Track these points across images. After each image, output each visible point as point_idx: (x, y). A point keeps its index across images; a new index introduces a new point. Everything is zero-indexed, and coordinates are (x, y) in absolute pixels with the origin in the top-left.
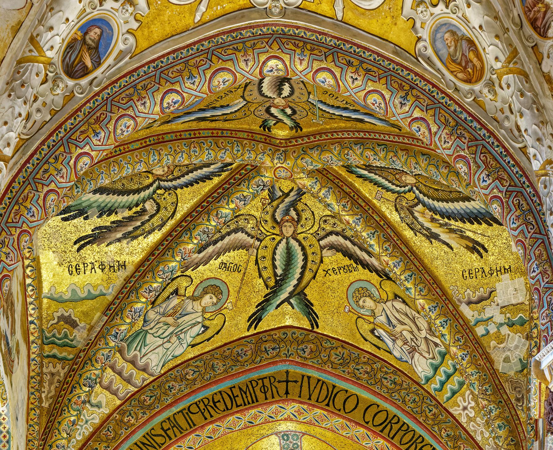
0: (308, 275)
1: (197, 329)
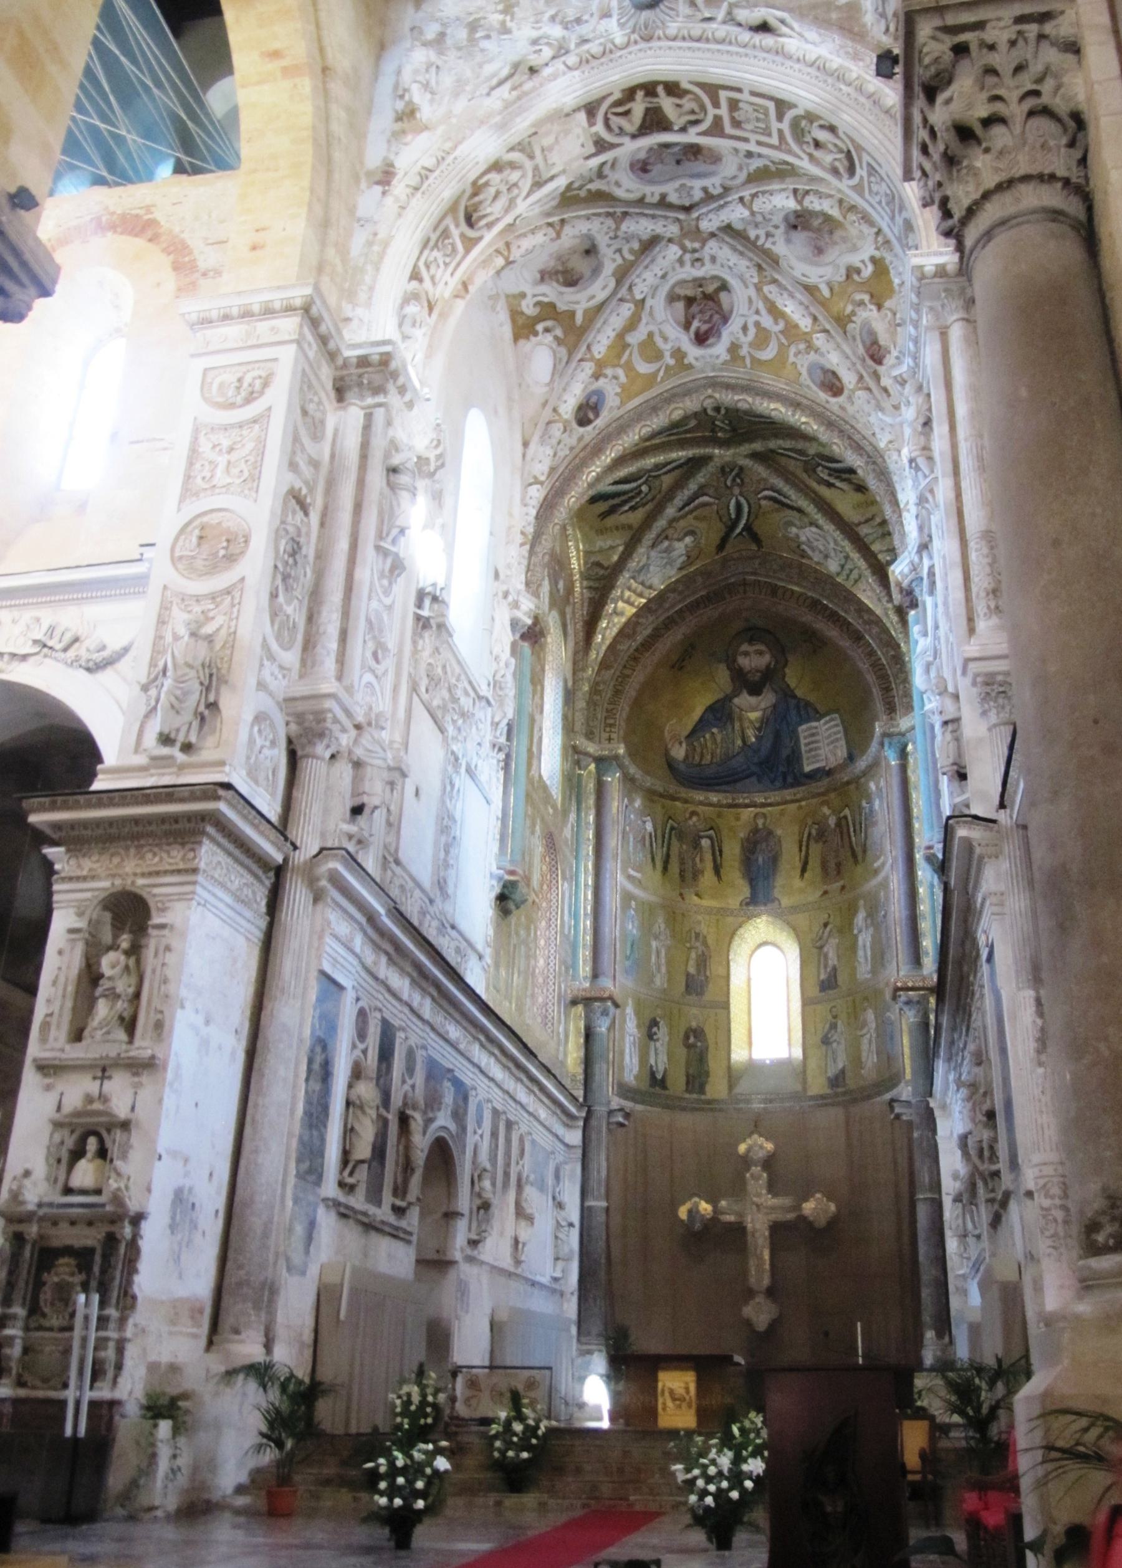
0: (752, 517)
1: (684, 558)
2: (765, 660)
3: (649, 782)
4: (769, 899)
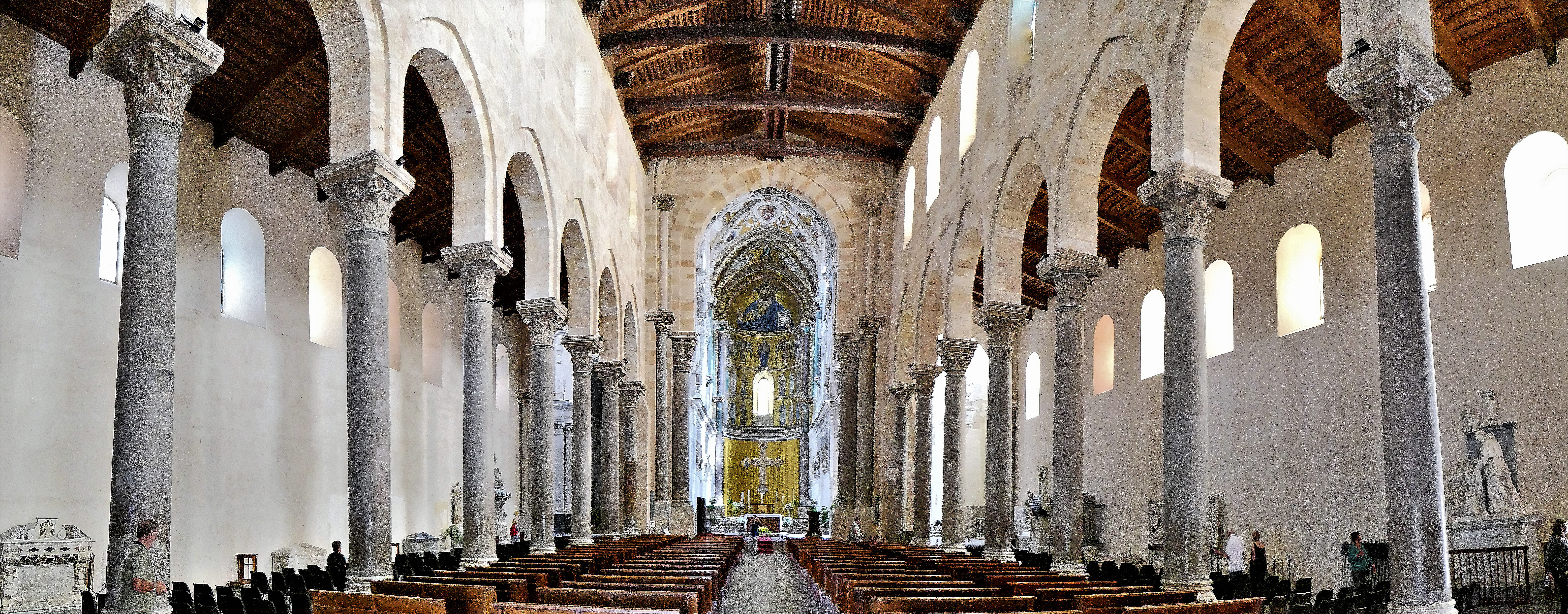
2: (770, 291)
3: (732, 329)
4: (766, 366)
